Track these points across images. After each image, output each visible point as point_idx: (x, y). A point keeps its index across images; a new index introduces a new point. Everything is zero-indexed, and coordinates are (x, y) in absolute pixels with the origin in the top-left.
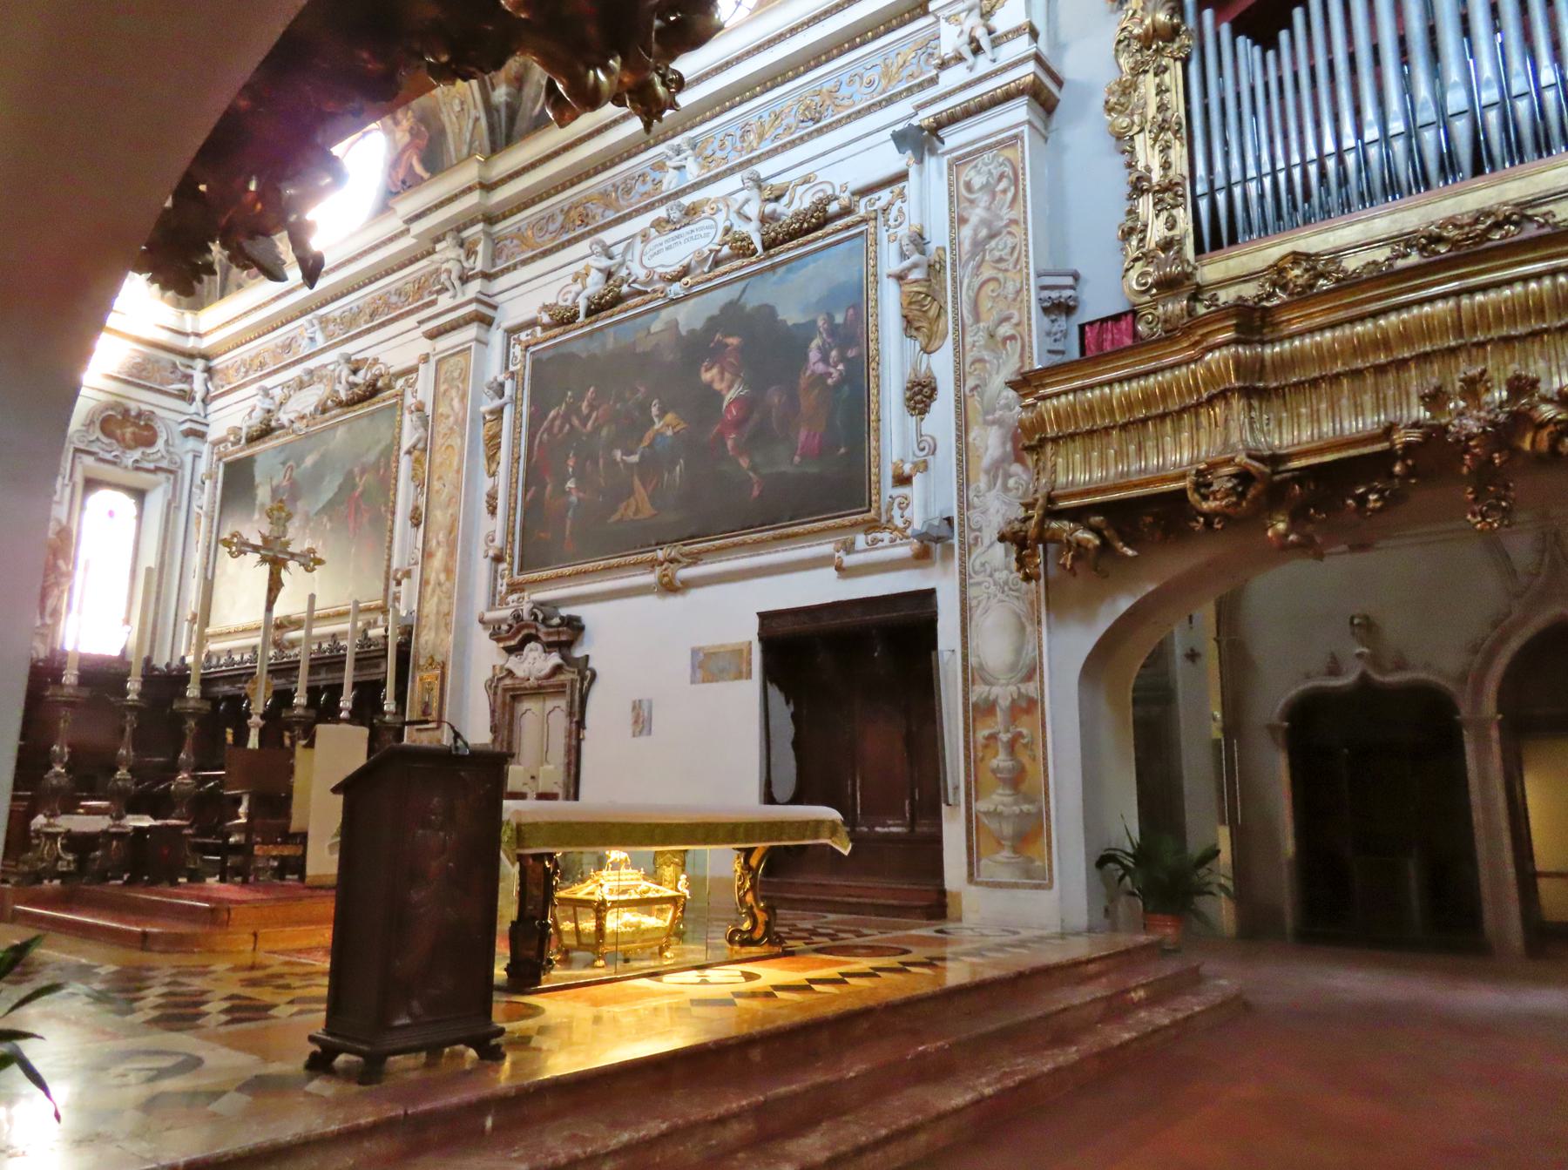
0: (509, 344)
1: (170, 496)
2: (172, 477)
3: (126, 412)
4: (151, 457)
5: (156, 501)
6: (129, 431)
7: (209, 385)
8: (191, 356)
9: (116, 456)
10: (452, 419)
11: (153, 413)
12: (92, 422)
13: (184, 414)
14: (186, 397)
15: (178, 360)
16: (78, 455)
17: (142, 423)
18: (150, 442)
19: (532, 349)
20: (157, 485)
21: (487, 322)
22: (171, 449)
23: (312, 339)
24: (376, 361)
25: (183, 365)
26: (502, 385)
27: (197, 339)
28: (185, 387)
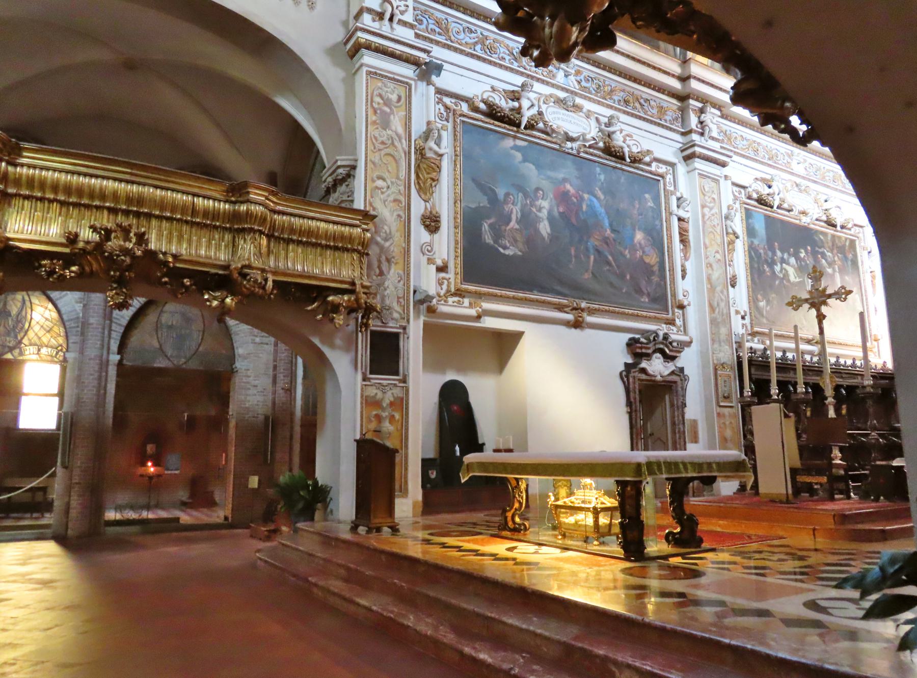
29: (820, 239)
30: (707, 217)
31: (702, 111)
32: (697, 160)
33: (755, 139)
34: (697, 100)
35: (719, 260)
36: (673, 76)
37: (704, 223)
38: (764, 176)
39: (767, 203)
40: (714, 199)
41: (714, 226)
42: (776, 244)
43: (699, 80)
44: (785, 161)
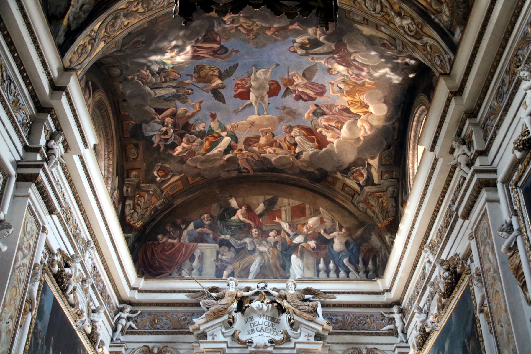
0: (509, 191)
7: (404, 320)
8: (389, 306)
10: (492, 270)
11: (376, 349)
13: (393, 344)
14: (393, 333)
15: (382, 311)
19: (520, 184)
23: (429, 262)
24: (456, 255)
25: (385, 313)
27: (388, 293)
28: (391, 326)
29: (80, 351)
30: (18, 264)
31: (52, 137)
32: (33, 186)
33: (71, 206)
34: (55, 120)
35: (9, 330)
36: (48, 74)
37: (14, 270)
38: (66, 251)
39: (62, 283)
40: (30, 245)
41: (20, 280)
42: (52, 339)
43: (69, 99)
44: (81, 247)
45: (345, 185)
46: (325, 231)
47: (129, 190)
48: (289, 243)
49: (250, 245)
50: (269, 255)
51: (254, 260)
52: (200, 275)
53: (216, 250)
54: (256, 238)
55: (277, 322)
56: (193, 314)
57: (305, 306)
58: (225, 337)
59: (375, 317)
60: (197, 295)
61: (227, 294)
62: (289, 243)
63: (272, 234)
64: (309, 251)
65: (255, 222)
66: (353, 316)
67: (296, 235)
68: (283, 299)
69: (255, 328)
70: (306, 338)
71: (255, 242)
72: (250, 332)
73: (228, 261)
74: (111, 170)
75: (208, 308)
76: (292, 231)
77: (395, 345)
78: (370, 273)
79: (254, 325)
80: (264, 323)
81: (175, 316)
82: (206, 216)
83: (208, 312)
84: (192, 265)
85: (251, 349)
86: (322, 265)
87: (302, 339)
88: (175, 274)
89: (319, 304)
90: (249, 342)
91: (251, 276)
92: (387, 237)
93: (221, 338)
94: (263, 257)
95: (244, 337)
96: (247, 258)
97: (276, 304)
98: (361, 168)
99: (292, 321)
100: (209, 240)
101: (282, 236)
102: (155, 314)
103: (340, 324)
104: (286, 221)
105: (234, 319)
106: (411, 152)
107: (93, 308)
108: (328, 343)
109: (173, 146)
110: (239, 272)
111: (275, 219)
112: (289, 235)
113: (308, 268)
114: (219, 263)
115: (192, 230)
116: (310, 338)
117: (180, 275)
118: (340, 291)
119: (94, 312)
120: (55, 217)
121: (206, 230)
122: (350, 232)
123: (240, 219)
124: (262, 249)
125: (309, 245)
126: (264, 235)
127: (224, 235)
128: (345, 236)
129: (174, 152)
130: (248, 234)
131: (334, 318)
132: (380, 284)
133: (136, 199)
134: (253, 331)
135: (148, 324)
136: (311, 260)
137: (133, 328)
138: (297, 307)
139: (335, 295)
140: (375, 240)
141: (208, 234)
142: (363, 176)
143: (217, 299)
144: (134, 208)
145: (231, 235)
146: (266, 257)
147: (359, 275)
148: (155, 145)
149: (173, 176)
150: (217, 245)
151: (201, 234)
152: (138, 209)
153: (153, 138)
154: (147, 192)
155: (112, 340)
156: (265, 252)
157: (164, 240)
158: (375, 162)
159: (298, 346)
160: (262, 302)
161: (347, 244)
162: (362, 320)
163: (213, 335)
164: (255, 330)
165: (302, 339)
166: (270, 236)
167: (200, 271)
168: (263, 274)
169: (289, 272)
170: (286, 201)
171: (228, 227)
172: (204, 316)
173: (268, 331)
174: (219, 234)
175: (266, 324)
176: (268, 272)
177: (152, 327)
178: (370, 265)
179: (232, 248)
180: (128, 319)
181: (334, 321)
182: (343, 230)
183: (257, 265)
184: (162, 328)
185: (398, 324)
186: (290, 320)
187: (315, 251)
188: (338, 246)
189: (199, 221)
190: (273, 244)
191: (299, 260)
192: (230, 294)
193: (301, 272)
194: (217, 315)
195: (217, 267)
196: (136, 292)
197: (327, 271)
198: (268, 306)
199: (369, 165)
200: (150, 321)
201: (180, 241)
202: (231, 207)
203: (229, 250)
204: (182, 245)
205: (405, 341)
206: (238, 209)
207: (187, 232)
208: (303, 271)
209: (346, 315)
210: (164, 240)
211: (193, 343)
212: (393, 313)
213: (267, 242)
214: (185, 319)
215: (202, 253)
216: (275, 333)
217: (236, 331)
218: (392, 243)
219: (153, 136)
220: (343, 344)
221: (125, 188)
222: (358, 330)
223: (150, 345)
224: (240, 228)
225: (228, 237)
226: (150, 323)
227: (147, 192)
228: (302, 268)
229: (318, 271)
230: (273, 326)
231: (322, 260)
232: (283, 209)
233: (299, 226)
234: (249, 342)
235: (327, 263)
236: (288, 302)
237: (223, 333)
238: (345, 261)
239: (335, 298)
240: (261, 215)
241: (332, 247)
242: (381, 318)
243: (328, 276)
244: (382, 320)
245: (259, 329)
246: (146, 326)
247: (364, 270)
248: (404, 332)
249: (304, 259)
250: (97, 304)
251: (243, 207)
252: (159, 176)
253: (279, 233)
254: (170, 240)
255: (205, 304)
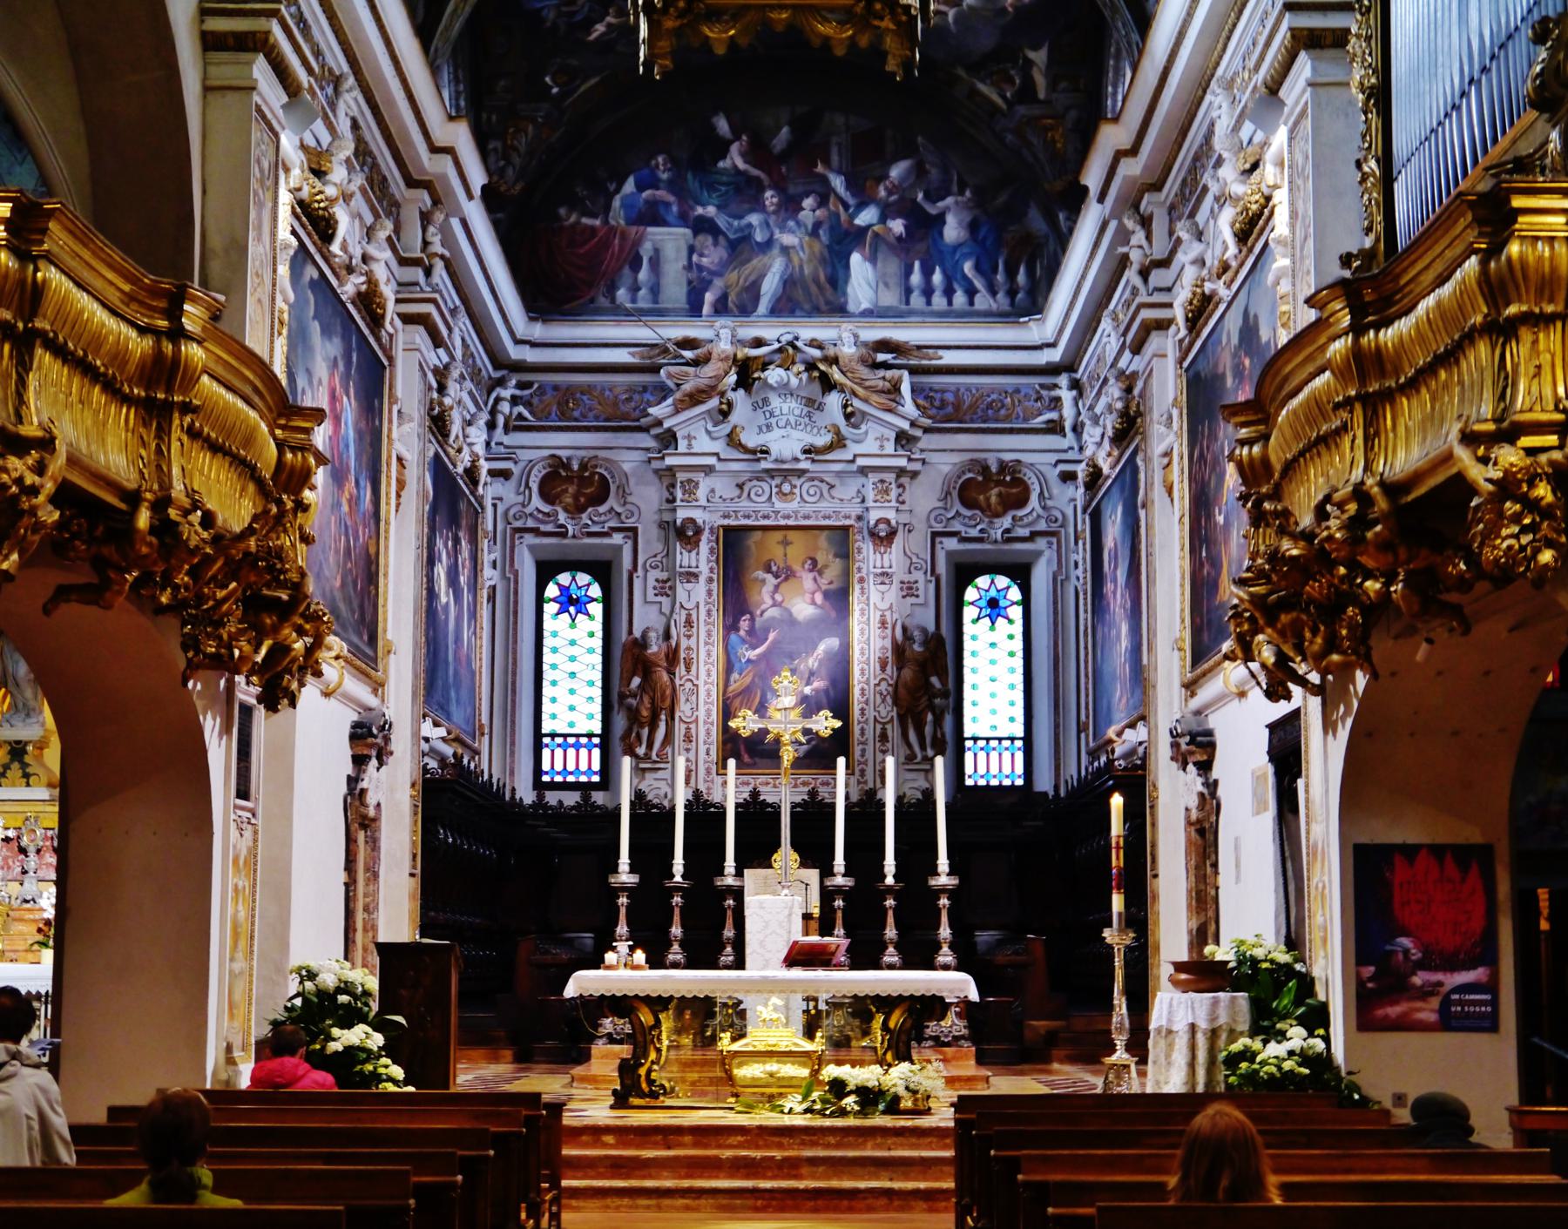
1: (1055, 568)
2: (1054, 540)
3: (985, 469)
4: (1026, 520)
5: (1040, 578)
6: (994, 494)
8: (1053, 370)
9: (982, 531)
11: (1019, 461)
12: (948, 493)
14: (1055, 428)
16: (938, 540)
17: (1008, 478)
18: (1022, 501)
20: (1039, 554)
21: (1163, 325)
22: (1049, 503)
26: (1170, 417)
28: (1053, 415)
39: (445, 426)
45: (974, 93)
46: (927, 197)
47: (494, 118)
48: (845, 225)
49: (761, 230)
50: (801, 254)
51: (770, 266)
52: (656, 301)
53: (687, 241)
54: (774, 213)
55: (818, 409)
56: (645, 389)
57: (877, 378)
58: (713, 439)
59: (1023, 393)
60: (652, 353)
61: (714, 355)
62: (845, 225)
63: (808, 202)
64: (891, 247)
65: (769, 174)
66: (977, 390)
67: (861, 206)
68: (831, 366)
69: (773, 421)
70: (878, 443)
71: (771, 223)
72: (764, 429)
73: (713, 268)
74: (462, 103)
75: (678, 385)
76: (853, 195)
77: (1055, 457)
78: (1020, 296)
79: (772, 415)
80: (791, 411)
81: (607, 393)
82: (660, 159)
83: (678, 395)
84: (636, 279)
85: (764, 465)
86: (916, 278)
87: (870, 446)
88: (603, 301)
89: (906, 373)
90: (762, 452)
91: (763, 306)
92: (1061, 216)
93: (703, 444)
94: (790, 260)
95: (751, 439)
96: (755, 262)
97: (816, 374)
98: (1009, 65)
99: (849, 409)
100: (670, 219)
101: (832, 207)
102: (567, 389)
103: (950, 409)
104: (839, 172)
105: (730, 404)
106: (1111, 62)
107: (468, 417)
108: (922, 451)
109: (588, 25)
110: (739, 294)
111: (816, 166)
112: (846, 206)
113: (886, 285)
114: (694, 275)
115: (632, 193)
116: (885, 443)
117: (613, 300)
118: (952, 343)
119: (470, 423)
120: (441, 351)
121: (662, 194)
122: (980, 201)
123: (735, 167)
124: (788, 239)
125: (890, 230)
126: (790, 206)
127: (704, 205)
128: (970, 209)
129: (590, 34)
130: (758, 206)
131: (938, 396)
132: (1035, 331)
133: (509, 137)
134: (769, 427)
135: (554, 408)
136: (893, 266)
137: (526, 419)
138: (861, 382)
139: (941, 352)
140: (1036, 221)
141: (668, 205)
142: (1013, 83)
143: (696, 363)
144: (506, 157)
145: (719, 207)
146: (796, 260)
147: (995, 300)
148: (548, 24)
149: (584, 81)
150: (688, 231)
151: (653, 204)
152: (517, 160)
153: (545, 12)
154: (533, 120)
155: (488, 444)
156: (794, 247)
157: (573, 219)
158: (1039, 57)
159: (861, 462)
160: (788, 369)
161: (973, 227)
162: (993, 401)
163: (689, 437)
164: (774, 425)
165: (870, 446)
166: (803, 209)
167: (655, 291)
168: (790, 299)
169: (845, 294)
170: (840, 120)
171: (711, 187)
172: (670, 401)
173: (801, 428)
174: (691, 202)
175: (797, 412)
176: (799, 294)
177: (563, 414)
178: (1021, 278)
179: (721, 239)
180: (515, 401)
181: (937, 403)
182: (968, 193)
183: (777, 277)
184: (584, 417)
185: (1068, 412)
186: (845, 406)
187: (902, 246)
188: (953, 231)
189: (646, 171)
190: (810, 227)
191: (868, 266)
192: (723, 356)
193: (870, 293)
194: (695, 398)
195: (690, 282)
196: (528, 347)
197: (928, 292)
198: (801, 379)
199: (1030, 63)
200: (559, 404)
201: (606, 222)
202: (717, 135)
203: (716, 244)
204: (612, 231)
205: (1076, 448)
206: (730, 142)
207: (622, 199)
208: (876, 292)
209: (962, 390)
210: (573, 219)
211: (647, 450)
212: (1056, 386)
213: (798, 223)
214: (629, 400)
215: (657, 251)
216: (815, 430)
217: (735, 427)
218: (1071, 231)
219: (543, 8)
220: (952, 451)
221: (484, 116)
222: (984, 422)
223: (563, 454)
224: (738, 190)
225: (711, 210)
226: (558, 408)
227: (533, 120)
228: (874, 285)
229: (908, 291)
230: (810, 417)
231: (917, 265)
232: (834, 140)
233: (868, 184)
234: (762, 452)
235: (927, 273)
236: (842, 372)
237: (708, 432)
238: (968, 267)
239: (940, 358)
240: (785, 156)
241: (941, 234)
242: (1034, 396)
243: (929, 303)
244: (1036, 401)
245: (782, 424)
246: (550, 414)
247: (1007, 287)
248: (1077, 429)
249: (879, 264)
250: (473, 409)
251: (744, 138)
252: (557, 85)
253: (823, 202)
254: (585, 220)
255: (670, 376)
